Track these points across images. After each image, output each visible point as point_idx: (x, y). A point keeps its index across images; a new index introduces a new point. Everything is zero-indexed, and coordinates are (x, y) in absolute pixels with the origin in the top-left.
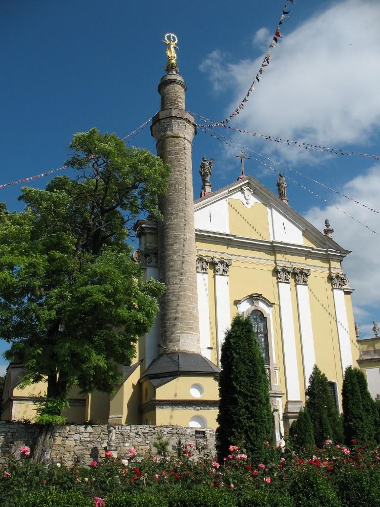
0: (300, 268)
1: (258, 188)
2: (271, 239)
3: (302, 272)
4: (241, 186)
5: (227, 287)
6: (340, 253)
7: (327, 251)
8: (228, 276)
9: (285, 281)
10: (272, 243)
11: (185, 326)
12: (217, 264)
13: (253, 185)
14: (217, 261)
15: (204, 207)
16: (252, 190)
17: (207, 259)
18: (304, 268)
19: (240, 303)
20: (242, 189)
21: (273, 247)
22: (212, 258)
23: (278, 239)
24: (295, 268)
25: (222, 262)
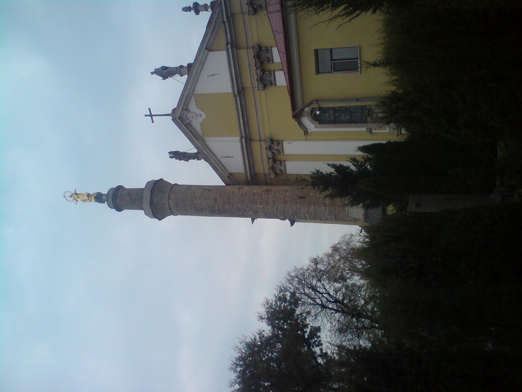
0: (253, 59)
1: (181, 108)
2: (230, 90)
3: (258, 56)
4: (186, 126)
5: (295, 143)
6: (221, 3)
7: (224, 22)
8: (282, 141)
9: (273, 78)
10: (235, 96)
11: (342, 214)
12: (273, 153)
13: (179, 113)
14: (270, 155)
15: (221, 163)
16: (186, 113)
17: (271, 165)
18: (253, 55)
19: (307, 129)
20: (189, 124)
21: (239, 93)
22: (269, 159)
23: (229, 84)
24: (255, 66)
25: (270, 148)
